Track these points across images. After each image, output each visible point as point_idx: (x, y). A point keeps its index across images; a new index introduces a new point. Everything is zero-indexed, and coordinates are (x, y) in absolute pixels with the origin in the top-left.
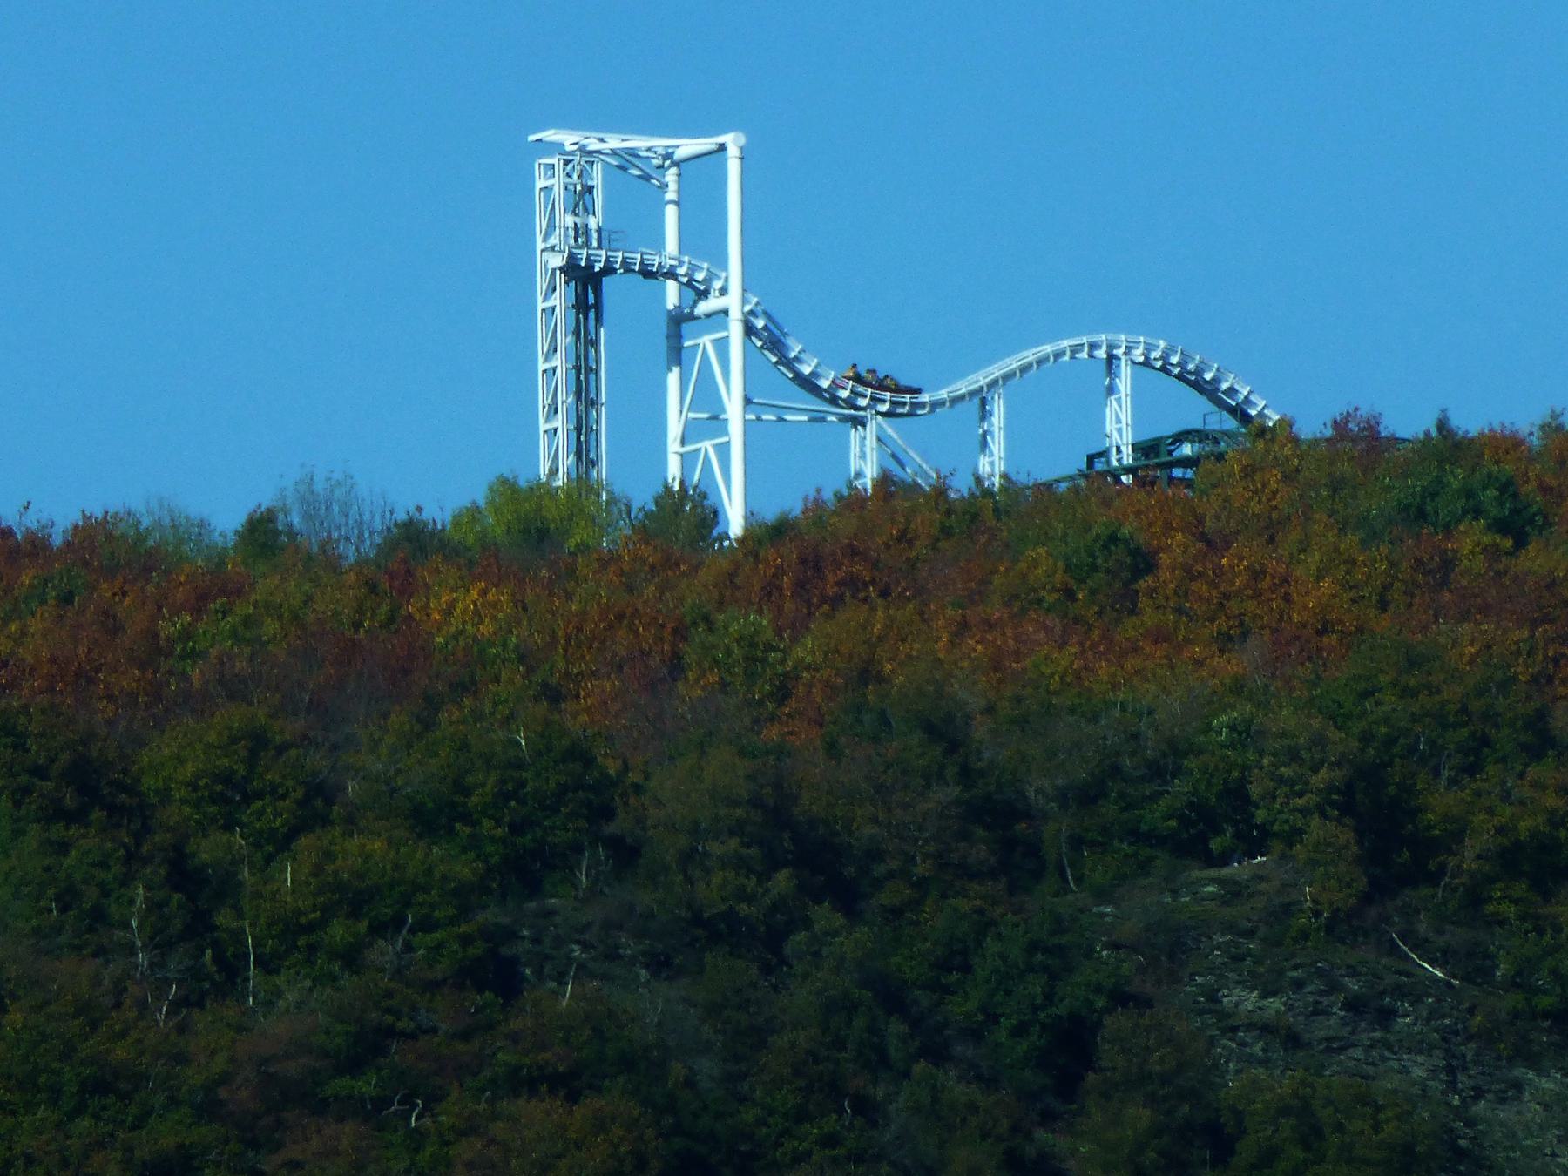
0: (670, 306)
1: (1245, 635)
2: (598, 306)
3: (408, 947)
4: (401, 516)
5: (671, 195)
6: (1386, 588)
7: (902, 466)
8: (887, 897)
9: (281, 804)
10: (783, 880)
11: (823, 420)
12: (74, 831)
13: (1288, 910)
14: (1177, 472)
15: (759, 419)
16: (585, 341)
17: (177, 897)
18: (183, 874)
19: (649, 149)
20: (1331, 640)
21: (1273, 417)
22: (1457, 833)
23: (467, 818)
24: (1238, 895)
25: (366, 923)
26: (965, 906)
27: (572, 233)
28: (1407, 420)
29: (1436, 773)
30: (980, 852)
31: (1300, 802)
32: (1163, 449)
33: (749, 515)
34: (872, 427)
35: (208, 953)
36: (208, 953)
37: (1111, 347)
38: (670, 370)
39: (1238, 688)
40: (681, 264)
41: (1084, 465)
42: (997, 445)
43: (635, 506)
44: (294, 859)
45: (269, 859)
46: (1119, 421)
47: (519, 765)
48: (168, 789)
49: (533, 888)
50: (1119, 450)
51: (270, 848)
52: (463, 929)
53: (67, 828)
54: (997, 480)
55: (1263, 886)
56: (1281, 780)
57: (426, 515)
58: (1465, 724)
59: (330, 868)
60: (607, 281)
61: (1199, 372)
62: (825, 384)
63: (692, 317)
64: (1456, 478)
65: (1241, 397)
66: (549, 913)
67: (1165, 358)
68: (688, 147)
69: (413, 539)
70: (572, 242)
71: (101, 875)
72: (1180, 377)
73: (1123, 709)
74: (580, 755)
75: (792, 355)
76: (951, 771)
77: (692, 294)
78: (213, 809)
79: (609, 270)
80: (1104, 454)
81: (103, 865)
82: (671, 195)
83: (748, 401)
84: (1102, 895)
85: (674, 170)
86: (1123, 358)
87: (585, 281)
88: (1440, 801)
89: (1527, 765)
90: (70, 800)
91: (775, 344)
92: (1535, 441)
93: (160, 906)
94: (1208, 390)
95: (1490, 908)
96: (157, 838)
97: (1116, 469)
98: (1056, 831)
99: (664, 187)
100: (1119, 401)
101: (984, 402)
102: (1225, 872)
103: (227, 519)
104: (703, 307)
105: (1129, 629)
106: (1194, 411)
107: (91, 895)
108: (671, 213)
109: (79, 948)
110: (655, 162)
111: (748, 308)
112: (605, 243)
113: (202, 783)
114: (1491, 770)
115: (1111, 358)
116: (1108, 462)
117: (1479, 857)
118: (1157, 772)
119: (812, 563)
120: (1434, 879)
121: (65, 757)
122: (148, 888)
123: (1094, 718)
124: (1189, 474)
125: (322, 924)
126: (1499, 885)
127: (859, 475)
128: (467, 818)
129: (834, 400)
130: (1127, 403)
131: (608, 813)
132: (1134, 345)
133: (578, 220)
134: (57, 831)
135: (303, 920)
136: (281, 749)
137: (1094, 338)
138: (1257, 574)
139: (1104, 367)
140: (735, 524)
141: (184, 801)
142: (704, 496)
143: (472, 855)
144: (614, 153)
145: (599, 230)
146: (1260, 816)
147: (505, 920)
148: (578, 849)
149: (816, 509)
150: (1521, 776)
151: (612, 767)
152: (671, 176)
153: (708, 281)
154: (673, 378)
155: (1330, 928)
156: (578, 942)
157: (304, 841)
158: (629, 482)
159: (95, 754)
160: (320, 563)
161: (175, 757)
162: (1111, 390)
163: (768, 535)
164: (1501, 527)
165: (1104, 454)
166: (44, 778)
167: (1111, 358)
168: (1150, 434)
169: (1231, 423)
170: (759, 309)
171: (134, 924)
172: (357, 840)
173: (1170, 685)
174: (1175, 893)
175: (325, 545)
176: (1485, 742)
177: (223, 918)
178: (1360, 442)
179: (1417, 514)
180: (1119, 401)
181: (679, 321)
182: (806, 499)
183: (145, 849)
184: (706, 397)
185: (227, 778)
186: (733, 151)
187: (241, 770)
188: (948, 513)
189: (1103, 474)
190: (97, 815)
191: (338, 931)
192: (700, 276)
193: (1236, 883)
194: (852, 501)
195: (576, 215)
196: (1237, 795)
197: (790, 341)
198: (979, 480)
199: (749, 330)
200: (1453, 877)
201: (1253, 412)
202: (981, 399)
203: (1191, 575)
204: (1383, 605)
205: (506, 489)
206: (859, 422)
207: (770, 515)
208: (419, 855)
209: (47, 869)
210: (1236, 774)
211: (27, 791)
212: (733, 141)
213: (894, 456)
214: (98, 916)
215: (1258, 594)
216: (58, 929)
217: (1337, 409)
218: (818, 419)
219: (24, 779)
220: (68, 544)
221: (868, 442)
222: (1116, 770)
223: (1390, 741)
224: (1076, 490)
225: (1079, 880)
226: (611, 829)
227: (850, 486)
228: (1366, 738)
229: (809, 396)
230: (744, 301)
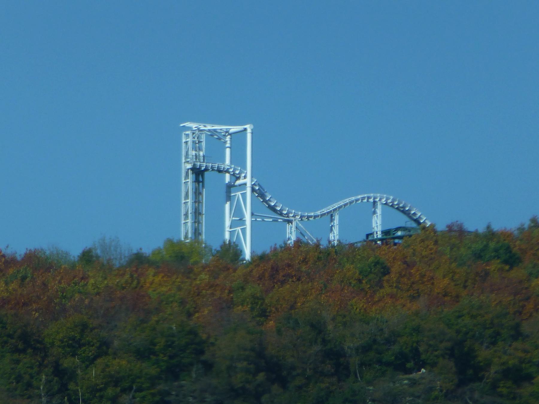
0: (227, 182)
1: (419, 296)
2: (203, 182)
3: (134, 398)
4: (135, 251)
5: (228, 145)
6: (466, 281)
7: (304, 236)
8: (298, 382)
9: (91, 348)
10: (261, 377)
11: (277, 221)
12: (22, 356)
13: (431, 389)
14: (396, 241)
15: (256, 220)
16: (197, 193)
17: (56, 378)
18: (58, 371)
19: (221, 129)
20: (447, 299)
21: (428, 224)
22: (489, 364)
23: (155, 354)
24: (415, 384)
25: (119, 388)
26: (323, 386)
27: (194, 157)
28: (475, 224)
29: (482, 343)
30: (328, 367)
31: (436, 353)
32: (392, 233)
33: (252, 252)
34: (294, 223)
35: (66, 398)
36: (66, 398)
37: (375, 198)
38: (226, 203)
39: (417, 314)
40: (231, 168)
41: (365, 238)
42: (336, 230)
43: (214, 248)
44: (95, 367)
45: (87, 367)
46: (377, 223)
47: (173, 336)
48: (53, 342)
49: (176, 377)
50: (377, 233)
51: (87, 363)
52: (152, 391)
53: (19, 355)
54: (336, 242)
55: (424, 381)
56: (430, 346)
57: (143, 251)
58: (491, 328)
59: (107, 370)
60: (206, 173)
61: (404, 207)
62: (279, 209)
63: (234, 186)
64: (492, 245)
65: (418, 216)
66: (182, 386)
67: (392, 202)
68: (234, 129)
69: (139, 260)
70: (194, 160)
71: (30, 371)
72: (397, 208)
73: (378, 320)
74: (193, 333)
75: (268, 199)
76: (319, 340)
77: (234, 178)
78: (68, 349)
79: (206, 170)
80: (372, 234)
81: (32, 368)
82: (228, 145)
83: (252, 214)
84: (369, 383)
85: (229, 137)
86: (379, 203)
87: (198, 173)
88: (483, 353)
89: (512, 342)
90: (21, 346)
91: (262, 195)
92: (516, 233)
93: (50, 381)
94: (406, 213)
95: (499, 390)
96: (49, 359)
97: (376, 239)
98: (355, 361)
99: (225, 142)
100: (377, 216)
101: (332, 216)
102: (411, 376)
103: (75, 252)
104: (238, 182)
105: (381, 292)
106: (402, 220)
107: (27, 377)
108: (228, 151)
109: (22, 396)
110: (223, 134)
111: (253, 183)
112: (205, 161)
113: (65, 340)
114: (500, 343)
115: (375, 202)
116: (373, 237)
117: (496, 372)
118: (389, 342)
119: (275, 270)
120: (480, 379)
121: (19, 331)
122: (46, 376)
123: (368, 323)
124: (400, 241)
125: (105, 389)
126: (502, 382)
127: (289, 239)
128: (155, 354)
129: (281, 214)
130: (380, 217)
131: (202, 352)
132: (382, 198)
133: (197, 153)
134: (16, 356)
135: (98, 387)
136: (92, 329)
137: (369, 195)
138: (422, 276)
139: (372, 204)
140: (247, 255)
141: (59, 347)
142: (237, 246)
143: (155, 366)
144: (209, 131)
145: (204, 156)
146: (423, 357)
147: (167, 388)
148: (192, 364)
149: (275, 250)
150: (510, 346)
151: (204, 337)
152: (228, 138)
153: (239, 174)
154: (227, 206)
155: (446, 395)
156: (191, 396)
157: (99, 361)
158: (211, 241)
159: (29, 330)
160: (106, 269)
161: (55, 332)
162: (374, 213)
163: (260, 259)
164: (506, 262)
165: (372, 234)
166: (12, 338)
167: (375, 202)
168: (387, 228)
169: (414, 225)
170: (257, 183)
171: (41, 388)
172: (117, 360)
173: (393, 312)
174: (394, 382)
175: (109, 260)
176: (498, 334)
177: (71, 386)
178: (457, 233)
179: (478, 256)
180: (377, 216)
181: (230, 187)
182: (271, 247)
183: (46, 362)
184: (238, 212)
185: (73, 339)
186: (249, 131)
187: (78, 336)
188: (320, 253)
189: (372, 241)
190: (30, 351)
191: (110, 392)
192: (237, 172)
193: (415, 380)
194: (286, 248)
195: (196, 151)
196: (416, 352)
197: (267, 194)
198: (330, 242)
199: (253, 190)
200: (487, 379)
201: (422, 221)
202: (331, 215)
203: (401, 276)
204: (465, 287)
205: (170, 243)
206: (290, 222)
207: (259, 252)
208: (138, 366)
209: (12, 369)
210: (415, 345)
211: (6, 342)
212: (249, 128)
213: (301, 233)
214: (29, 385)
215: (423, 283)
216: (16, 389)
217: (449, 222)
218: (275, 220)
219: (5, 338)
220: (23, 259)
221: (293, 228)
222: (375, 341)
223: (467, 333)
224: (363, 246)
225: (361, 378)
226: (203, 358)
227: (285, 244)
228: (458, 332)
229: (272, 212)
230: (252, 181)
